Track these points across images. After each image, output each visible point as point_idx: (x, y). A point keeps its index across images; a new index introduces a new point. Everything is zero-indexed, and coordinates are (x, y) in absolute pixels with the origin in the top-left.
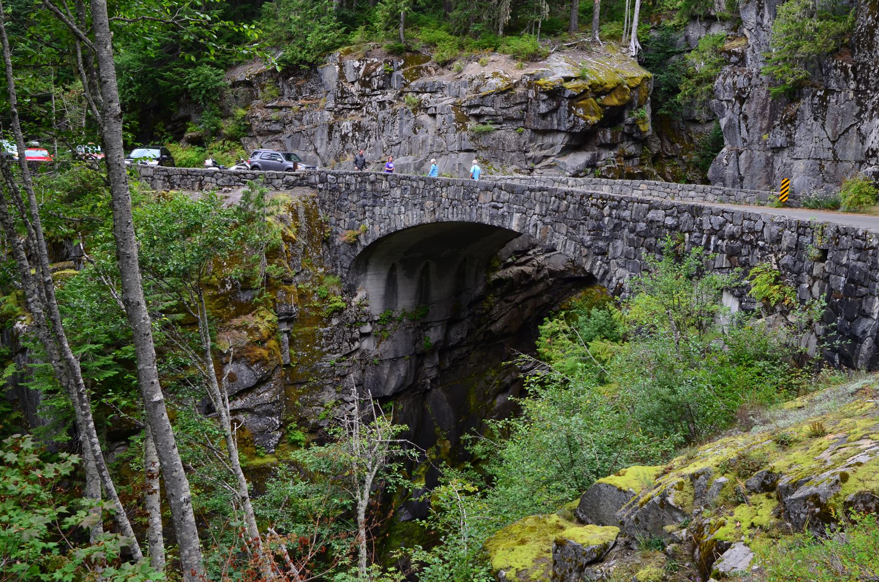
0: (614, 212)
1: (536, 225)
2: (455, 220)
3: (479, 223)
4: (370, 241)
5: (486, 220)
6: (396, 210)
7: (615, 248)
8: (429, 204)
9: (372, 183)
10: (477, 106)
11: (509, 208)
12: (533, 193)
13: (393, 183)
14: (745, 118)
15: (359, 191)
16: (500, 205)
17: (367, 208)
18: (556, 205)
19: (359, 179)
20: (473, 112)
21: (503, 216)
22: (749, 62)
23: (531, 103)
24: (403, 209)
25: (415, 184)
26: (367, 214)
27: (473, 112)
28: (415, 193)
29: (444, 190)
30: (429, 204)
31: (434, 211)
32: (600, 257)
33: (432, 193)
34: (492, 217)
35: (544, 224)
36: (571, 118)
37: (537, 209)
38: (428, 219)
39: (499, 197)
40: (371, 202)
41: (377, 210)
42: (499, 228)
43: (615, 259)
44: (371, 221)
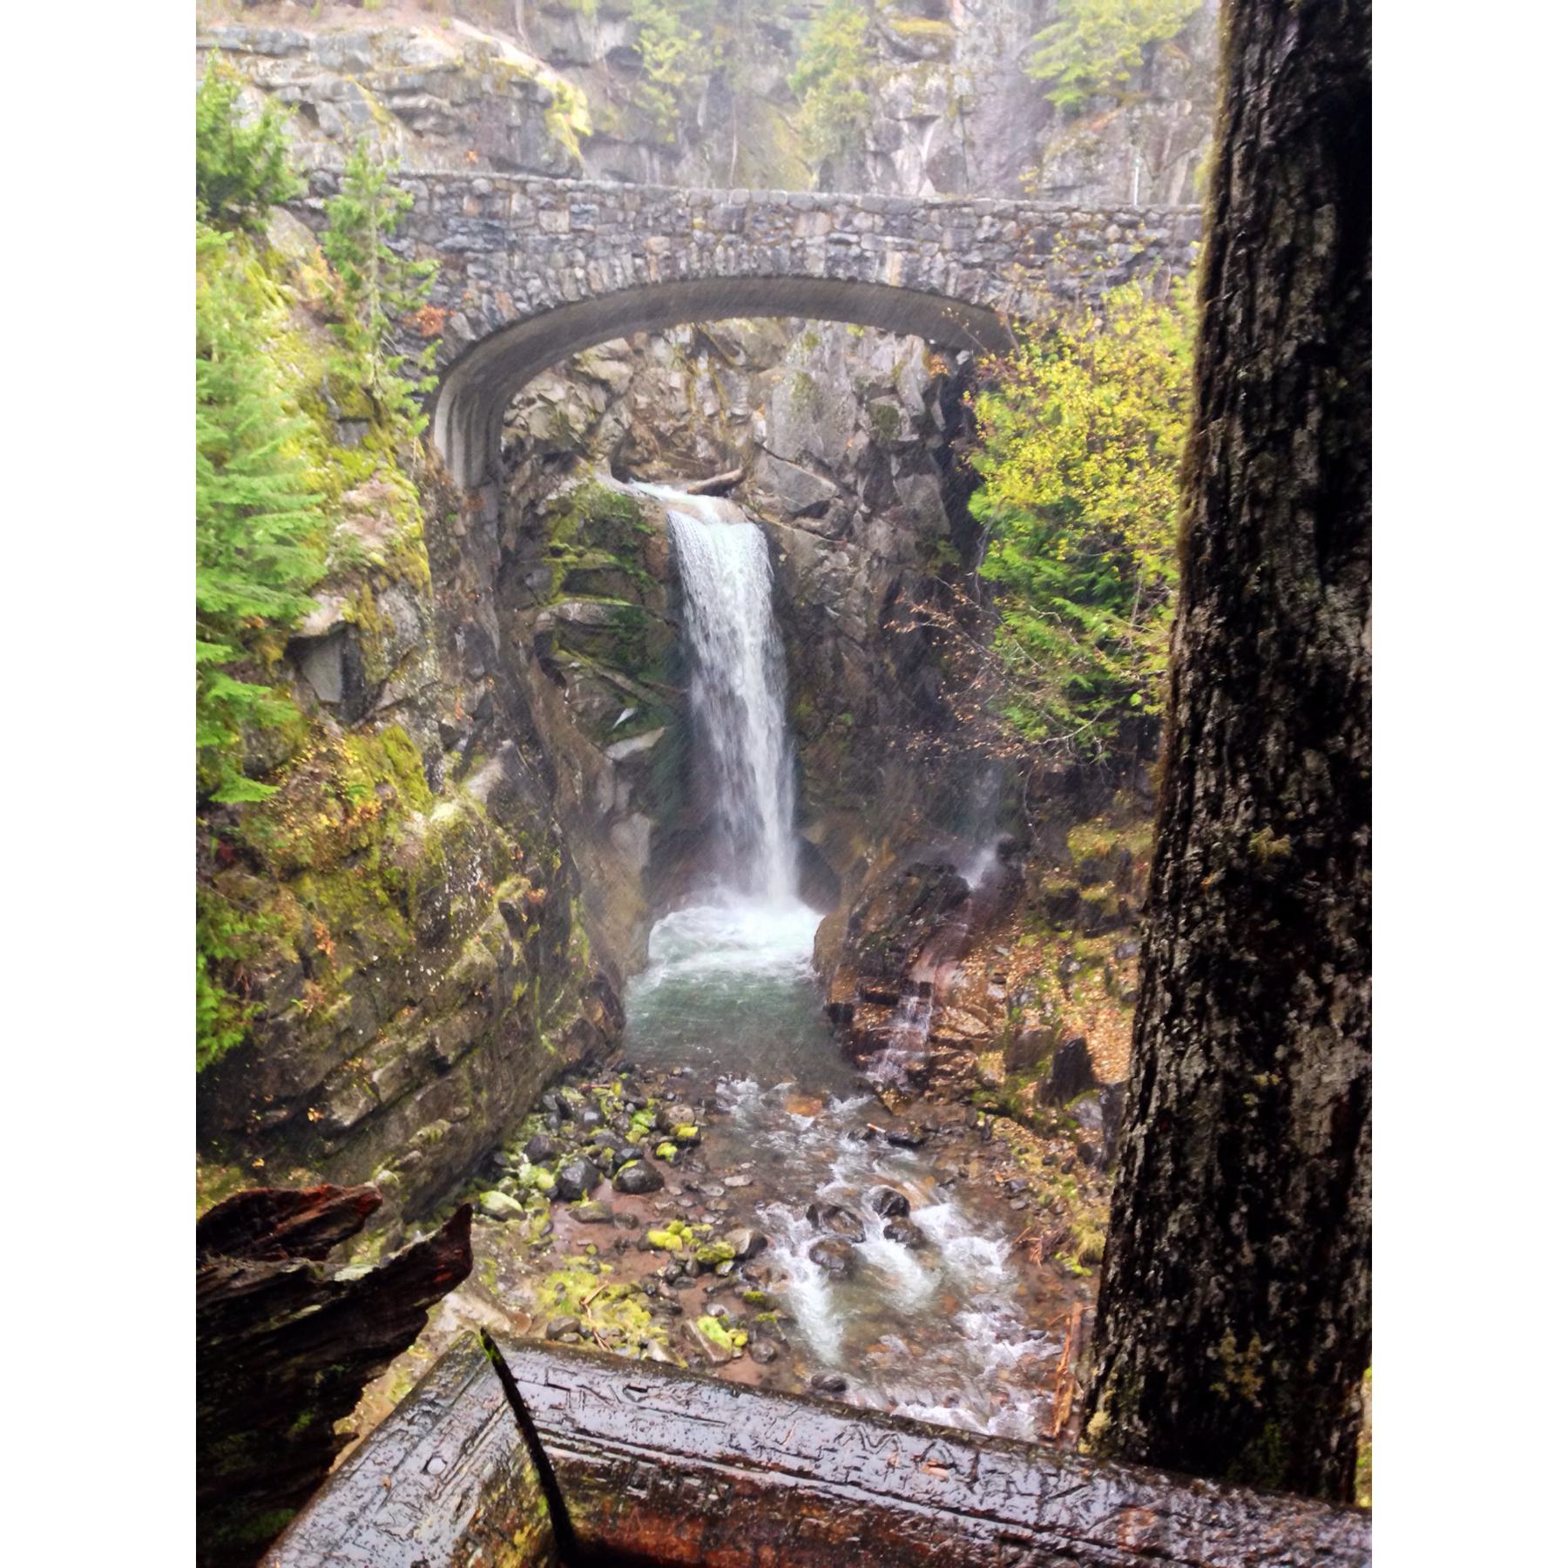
1: (946, 273)
2: (733, 272)
5: (819, 269)
8: (657, 243)
9: (481, 197)
10: (413, 91)
12: (935, 213)
14: (973, 145)
16: (853, 238)
17: (469, 254)
18: (993, 231)
19: (440, 189)
20: (398, 101)
21: (861, 258)
22: (958, 55)
24: (580, 256)
26: (471, 269)
27: (398, 101)
34: (834, 262)
35: (966, 266)
38: (653, 275)
39: (847, 222)
42: (852, 280)
44: (484, 284)
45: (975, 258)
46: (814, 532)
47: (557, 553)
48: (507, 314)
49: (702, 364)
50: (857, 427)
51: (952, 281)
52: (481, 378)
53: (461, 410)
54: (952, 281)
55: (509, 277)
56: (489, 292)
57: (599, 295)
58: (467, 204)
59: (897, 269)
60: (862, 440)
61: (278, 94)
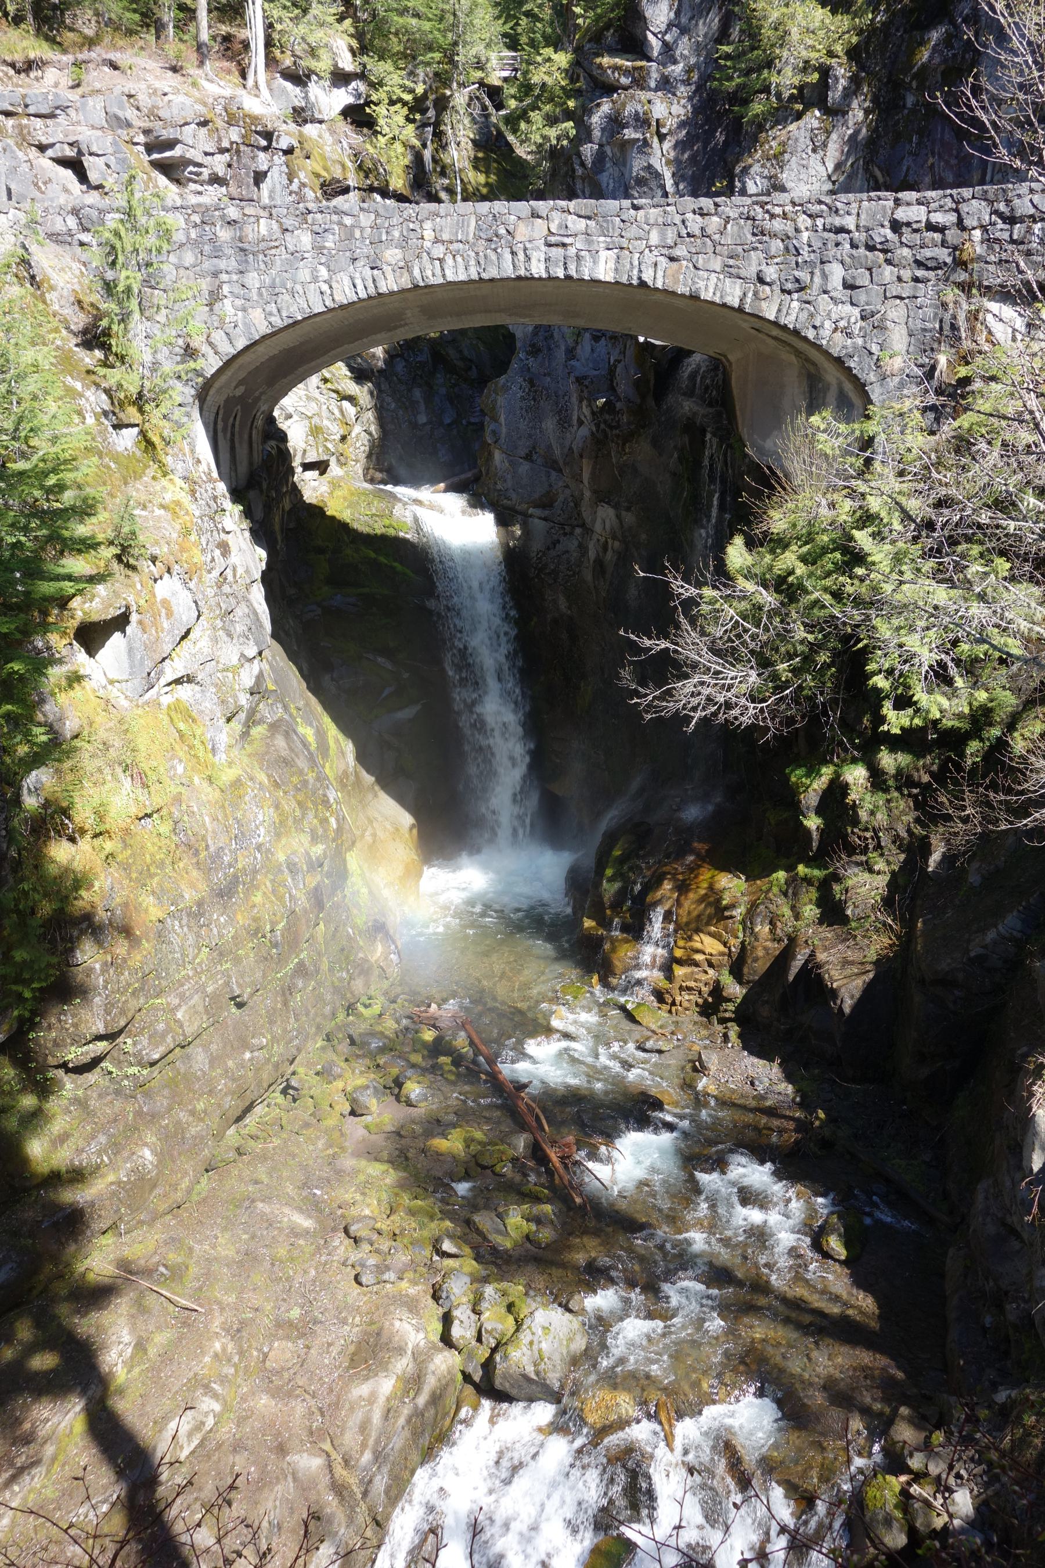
0: (820, 222)
2: (462, 277)
3: (519, 278)
4: (241, 344)
5: (538, 269)
6: (304, 275)
7: (825, 276)
11: (590, 243)
13: (288, 222)
15: (196, 243)
16: (567, 240)
17: (224, 277)
23: (238, 151)
24: (323, 272)
25: (348, 221)
28: (351, 236)
29: (428, 225)
30: (393, 255)
31: (408, 268)
32: (795, 296)
33: (396, 234)
35: (672, 259)
36: (295, 187)
37: (654, 238)
38: (390, 283)
39: (560, 227)
40: (233, 264)
41: (253, 279)
43: (825, 292)
44: (239, 302)
45: (680, 251)
46: (545, 519)
47: (321, 551)
48: (264, 329)
49: (440, 378)
50: (581, 423)
51: (660, 274)
52: (242, 389)
53: (225, 421)
54: (660, 274)
55: (260, 295)
56: (244, 310)
57: (342, 307)
58: (224, 234)
59: (611, 265)
60: (584, 431)
61: (50, 153)
